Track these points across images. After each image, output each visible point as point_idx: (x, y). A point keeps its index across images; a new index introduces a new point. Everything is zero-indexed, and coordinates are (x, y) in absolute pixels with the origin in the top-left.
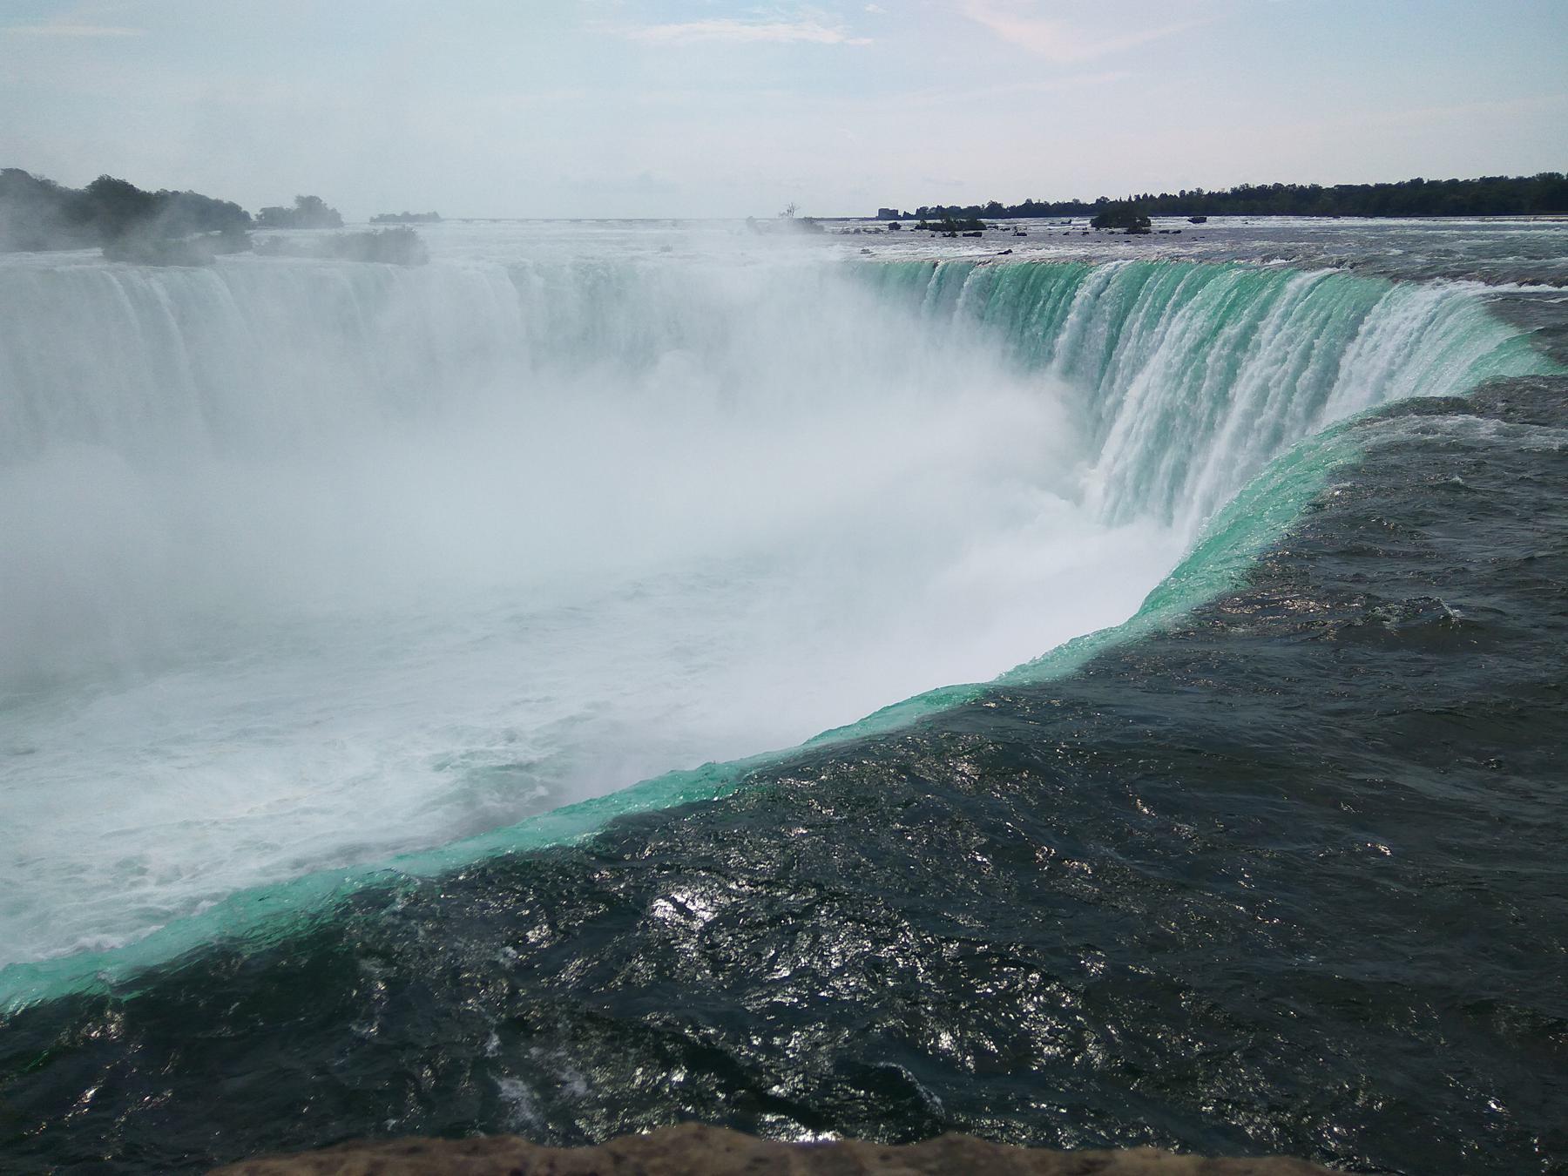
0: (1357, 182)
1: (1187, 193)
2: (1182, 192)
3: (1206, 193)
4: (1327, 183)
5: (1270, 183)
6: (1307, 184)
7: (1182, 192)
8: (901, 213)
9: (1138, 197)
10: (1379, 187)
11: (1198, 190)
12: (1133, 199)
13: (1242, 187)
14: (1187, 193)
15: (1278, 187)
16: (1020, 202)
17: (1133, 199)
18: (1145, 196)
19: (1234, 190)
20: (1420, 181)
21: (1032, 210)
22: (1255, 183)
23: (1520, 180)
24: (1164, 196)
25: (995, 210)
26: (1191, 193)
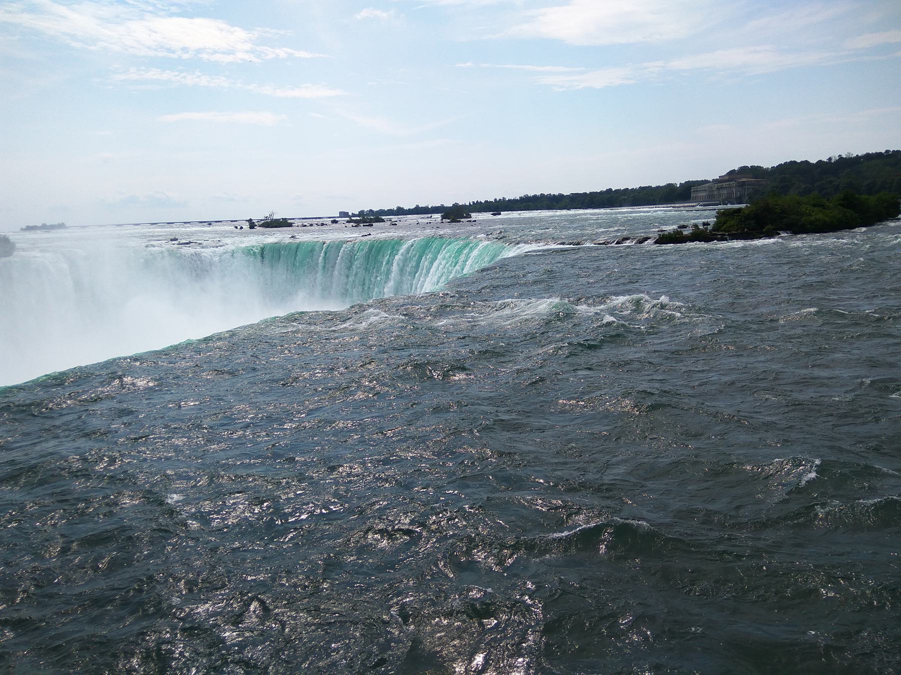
1: (498, 200)
2: (495, 199)
3: (507, 199)
4: (566, 192)
5: (538, 194)
6: (556, 193)
7: (495, 199)
8: (350, 214)
11: (503, 198)
12: (472, 204)
13: (525, 196)
14: (498, 200)
15: (542, 195)
17: (472, 204)
18: (477, 201)
19: (521, 198)
20: (611, 189)
21: (418, 211)
22: (531, 194)
23: (658, 187)
25: (400, 211)
26: (500, 199)
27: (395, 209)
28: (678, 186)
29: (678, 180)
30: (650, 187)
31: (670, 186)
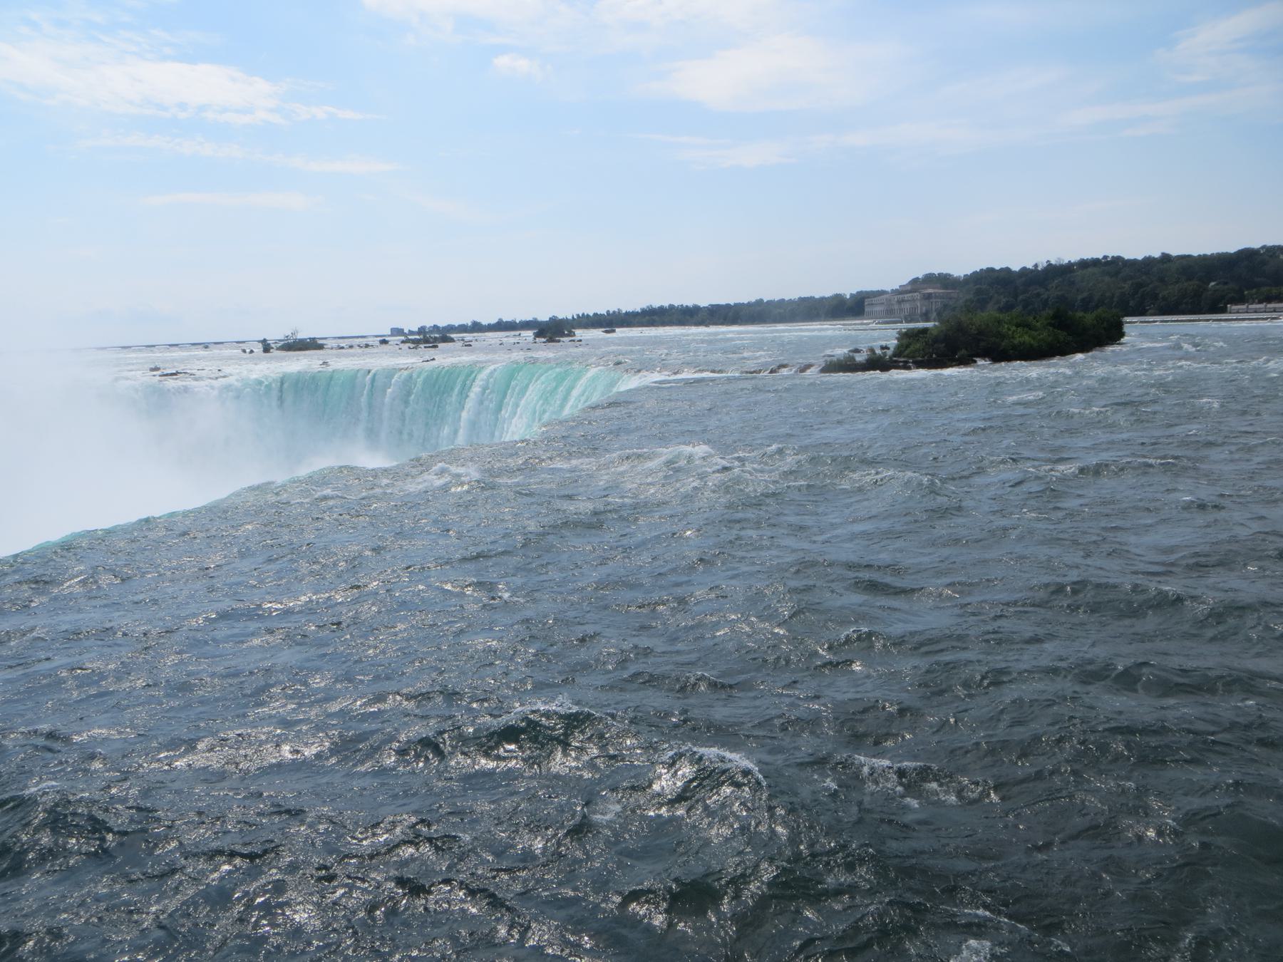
0: (722, 301)
1: (611, 312)
3: (624, 312)
4: (704, 303)
5: (666, 304)
8: (406, 331)
10: (736, 305)
12: (575, 317)
14: (611, 312)
15: (671, 307)
16: (494, 321)
17: (575, 317)
18: (583, 314)
20: (761, 300)
21: (501, 326)
22: (656, 304)
23: (822, 299)
24: (595, 315)
25: (477, 327)
26: (614, 312)
27: (470, 324)
28: (848, 297)
30: (812, 298)
31: (838, 299)
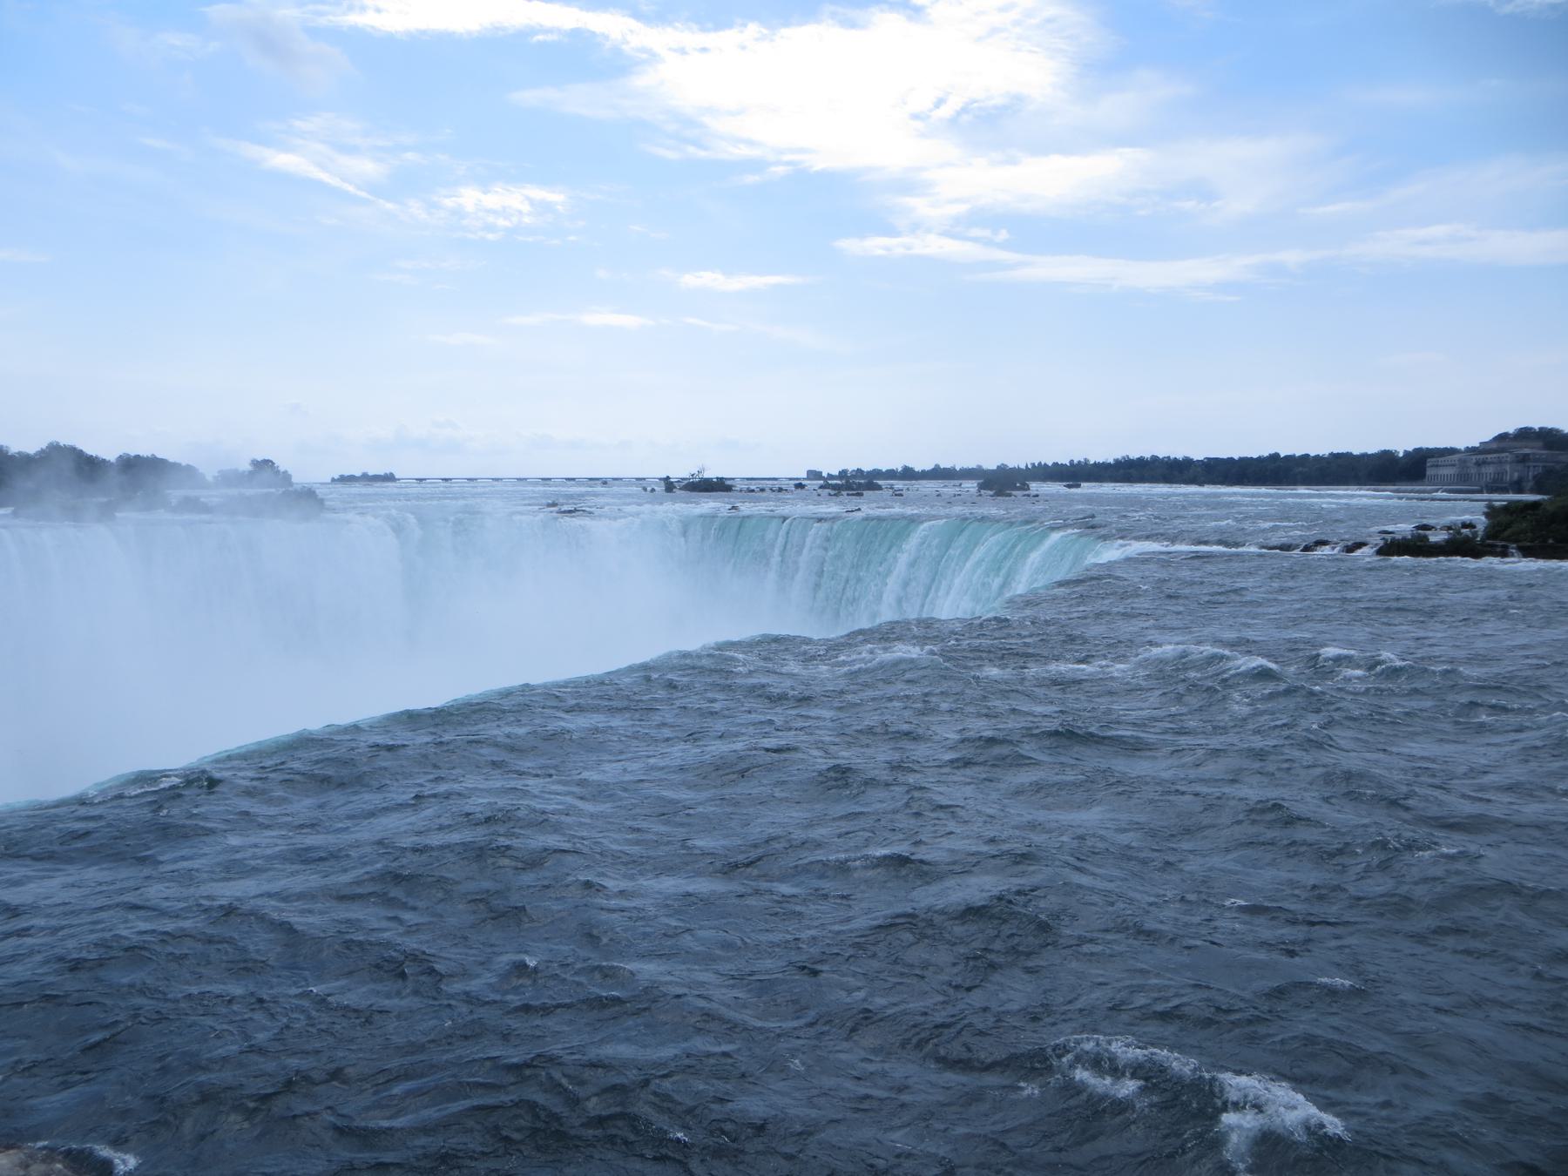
0: (1223, 453)
1: (1075, 462)
2: (1072, 461)
3: (1092, 462)
4: (1198, 455)
5: (1147, 455)
6: (1180, 456)
7: (1072, 461)
8: (825, 475)
9: (1033, 464)
10: (1242, 460)
12: (1030, 466)
13: (1124, 458)
14: (1075, 462)
15: (1155, 459)
16: (929, 466)
17: (1030, 466)
18: (1040, 463)
21: (938, 474)
22: (1134, 455)
23: (1364, 456)
24: (1056, 464)
25: (908, 474)
26: (1079, 462)
27: (900, 469)
29: (1402, 443)
30: (1348, 456)
31: (1387, 457)
